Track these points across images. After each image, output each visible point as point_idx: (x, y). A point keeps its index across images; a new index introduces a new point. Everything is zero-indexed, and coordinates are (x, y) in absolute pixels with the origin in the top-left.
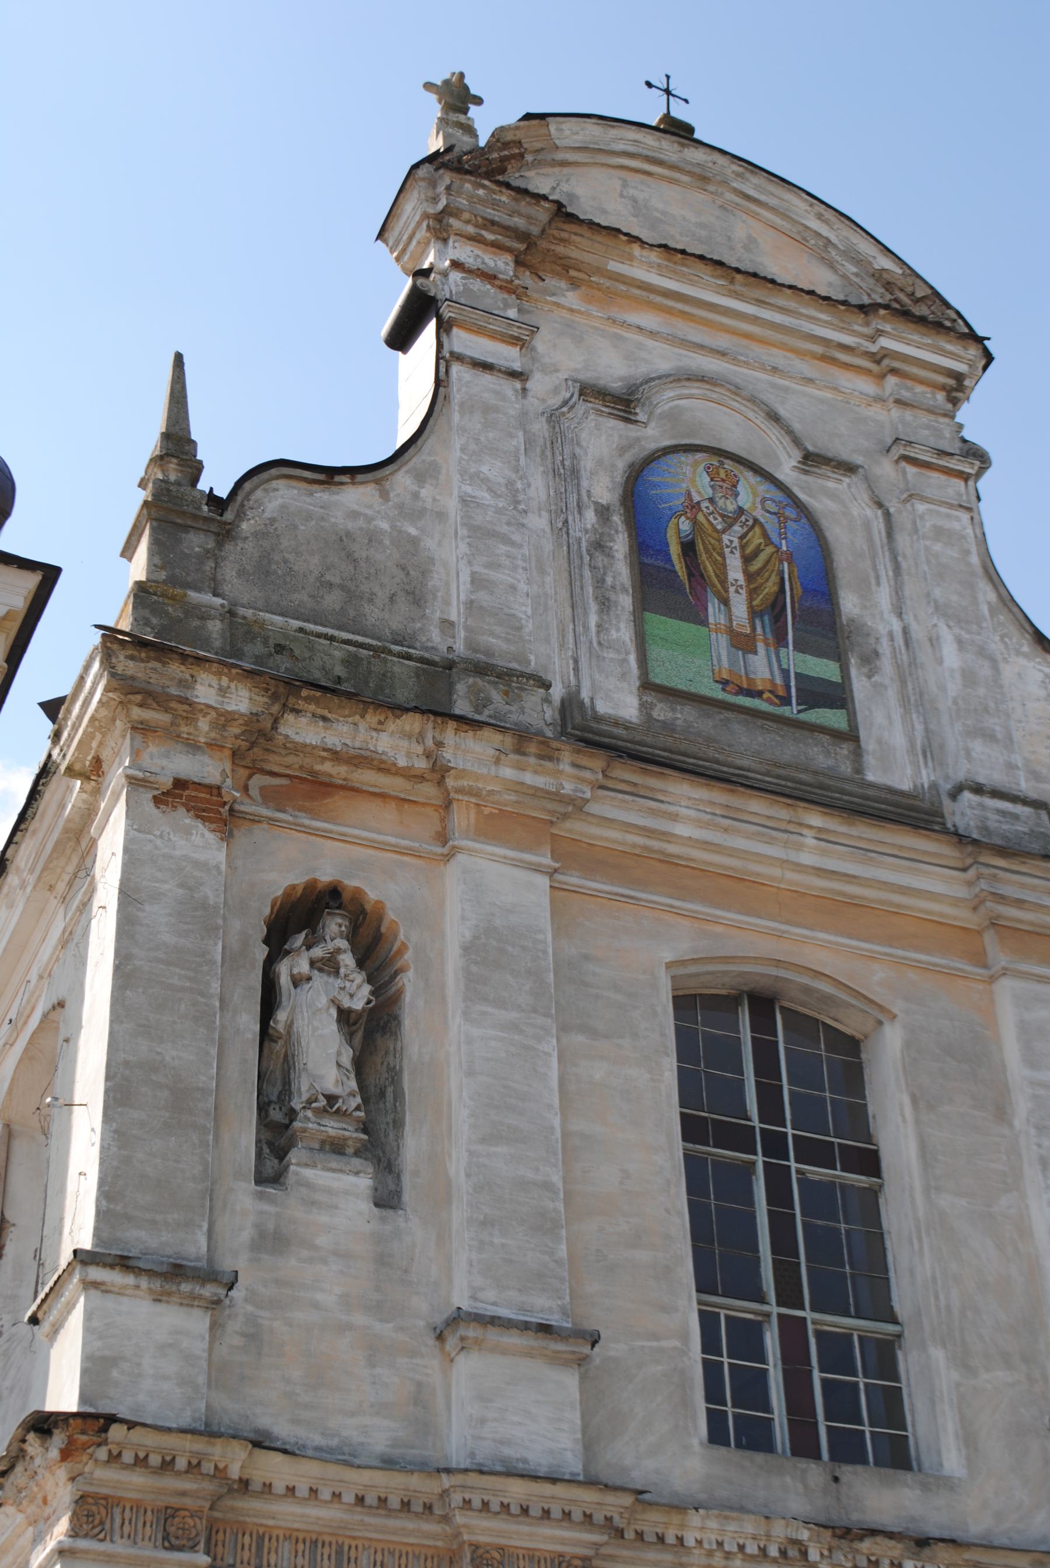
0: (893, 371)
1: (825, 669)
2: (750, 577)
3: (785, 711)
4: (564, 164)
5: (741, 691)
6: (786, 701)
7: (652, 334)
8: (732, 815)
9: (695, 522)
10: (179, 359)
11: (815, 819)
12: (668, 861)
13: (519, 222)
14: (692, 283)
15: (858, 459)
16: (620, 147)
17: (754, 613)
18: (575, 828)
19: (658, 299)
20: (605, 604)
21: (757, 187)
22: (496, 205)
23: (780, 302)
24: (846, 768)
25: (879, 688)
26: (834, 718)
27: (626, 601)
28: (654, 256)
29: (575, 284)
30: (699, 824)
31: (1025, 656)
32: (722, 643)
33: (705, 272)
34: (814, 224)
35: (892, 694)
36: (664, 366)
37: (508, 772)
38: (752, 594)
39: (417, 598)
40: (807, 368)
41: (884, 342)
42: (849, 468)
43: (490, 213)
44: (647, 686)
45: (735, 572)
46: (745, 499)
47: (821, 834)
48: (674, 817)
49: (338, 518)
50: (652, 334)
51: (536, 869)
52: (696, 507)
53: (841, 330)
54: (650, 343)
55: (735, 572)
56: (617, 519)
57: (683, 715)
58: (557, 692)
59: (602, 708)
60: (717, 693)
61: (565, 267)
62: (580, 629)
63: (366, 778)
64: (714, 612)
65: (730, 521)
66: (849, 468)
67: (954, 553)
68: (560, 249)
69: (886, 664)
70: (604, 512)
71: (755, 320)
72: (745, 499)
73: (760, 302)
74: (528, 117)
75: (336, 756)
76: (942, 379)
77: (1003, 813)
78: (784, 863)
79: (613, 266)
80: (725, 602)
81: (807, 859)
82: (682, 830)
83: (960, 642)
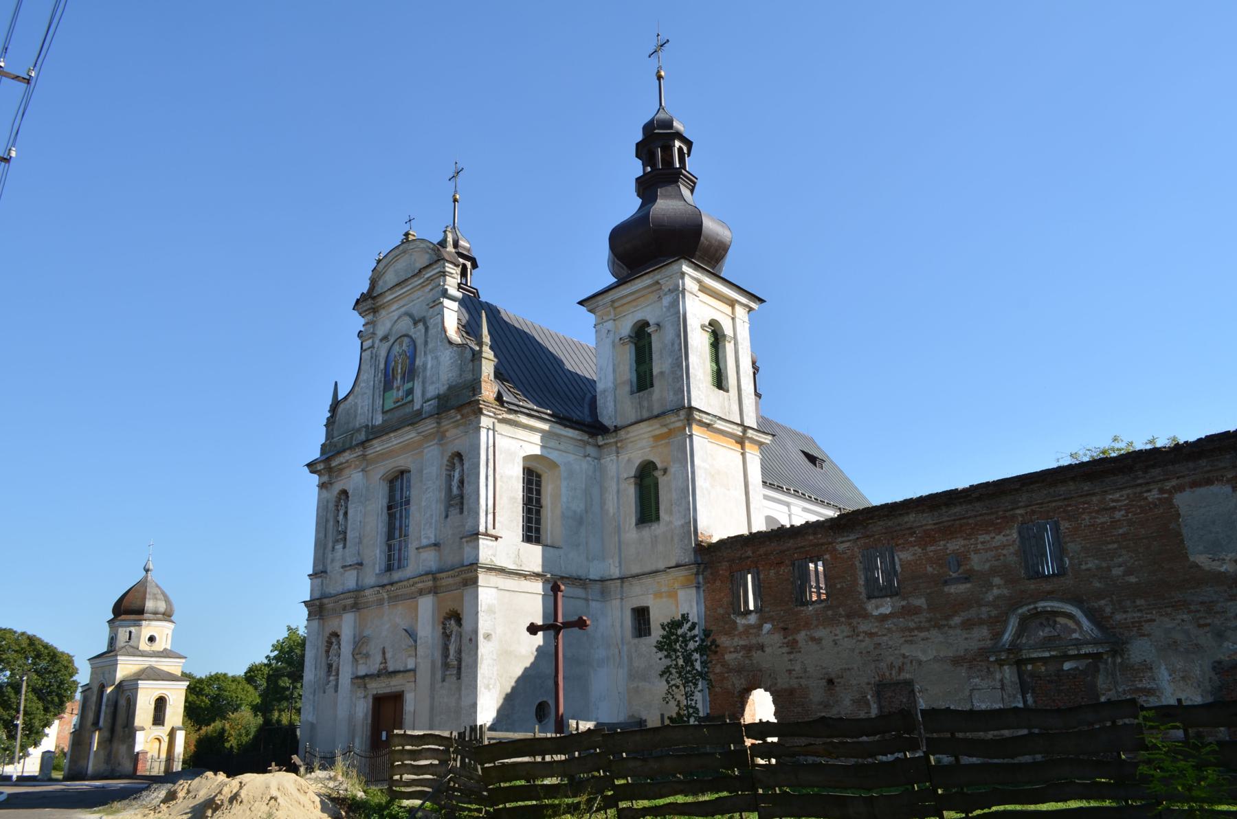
0: (432, 280)
1: (410, 385)
2: (401, 369)
3: (404, 401)
4: (384, 273)
5: (397, 402)
6: (403, 399)
7: (394, 311)
8: (383, 441)
9: (395, 361)
10: (336, 383)
11: (392, 435)
12: (382, 454)
13: (368, 307)
14: (396, 292)
15: (425, 314)
16: (391, 258)
17: (401, 379)
18: (368, 457)
19: (395, 300)
20: (380, 397)
21: (413, 245)
22: (364, 306)
23: (409, 283)
24: (411, 410)
25: (419, 382)
26: (410, 398)
27: (382, 393)
28: (389, 292)
29: (384, 308)
30: (380, 446)
31: (447, 349)
32: (395, 391)
33: (397, 289)
34: (422, 245)
35: (420, 383)
36: (396, 318)
37: (352, 456)
38: (401, 372)
39: (355, 417)
40: (419, 293)
41: (426, 276)
42: (420, 321)
43: (365, 309)
44: (384, 412)
45: (399, 371)
46: (403, 348)
47: (395, 437)
48: (376, 448)
49: (348, 407)
50: (394, 311)
51: (359, 472)
52: (395, 356)
53: (421, 279)
54: (393, 313)
55: (399, 371)
56: (383, 371)
57: (389, 415)
58: (370, 424)
59: (377, 424)
60: (393, 406)
61: (383, 307)
62: (374, 406)
63: (344, 465)
64: (395, 385)
65: (400, 355)
66: (420, 321)
67: (435, 330)
68: (378, 304)
69: (421, 376)
70: (382, 373)
71: (408, 290)
72: (403, 348)
73: (407, 286)
74: (373, 271)
75: (339, 465)
76: (438, 275)
77: (429, 405)
78: (393, 446)
79: (385, 301)
80: (397, 380)
81: (395, 443)
82: (378, 449)
83: (432, 358)
